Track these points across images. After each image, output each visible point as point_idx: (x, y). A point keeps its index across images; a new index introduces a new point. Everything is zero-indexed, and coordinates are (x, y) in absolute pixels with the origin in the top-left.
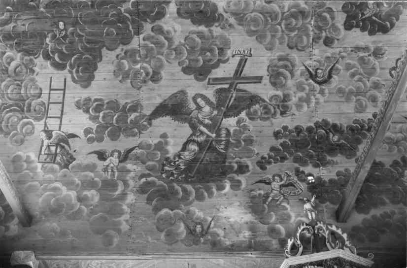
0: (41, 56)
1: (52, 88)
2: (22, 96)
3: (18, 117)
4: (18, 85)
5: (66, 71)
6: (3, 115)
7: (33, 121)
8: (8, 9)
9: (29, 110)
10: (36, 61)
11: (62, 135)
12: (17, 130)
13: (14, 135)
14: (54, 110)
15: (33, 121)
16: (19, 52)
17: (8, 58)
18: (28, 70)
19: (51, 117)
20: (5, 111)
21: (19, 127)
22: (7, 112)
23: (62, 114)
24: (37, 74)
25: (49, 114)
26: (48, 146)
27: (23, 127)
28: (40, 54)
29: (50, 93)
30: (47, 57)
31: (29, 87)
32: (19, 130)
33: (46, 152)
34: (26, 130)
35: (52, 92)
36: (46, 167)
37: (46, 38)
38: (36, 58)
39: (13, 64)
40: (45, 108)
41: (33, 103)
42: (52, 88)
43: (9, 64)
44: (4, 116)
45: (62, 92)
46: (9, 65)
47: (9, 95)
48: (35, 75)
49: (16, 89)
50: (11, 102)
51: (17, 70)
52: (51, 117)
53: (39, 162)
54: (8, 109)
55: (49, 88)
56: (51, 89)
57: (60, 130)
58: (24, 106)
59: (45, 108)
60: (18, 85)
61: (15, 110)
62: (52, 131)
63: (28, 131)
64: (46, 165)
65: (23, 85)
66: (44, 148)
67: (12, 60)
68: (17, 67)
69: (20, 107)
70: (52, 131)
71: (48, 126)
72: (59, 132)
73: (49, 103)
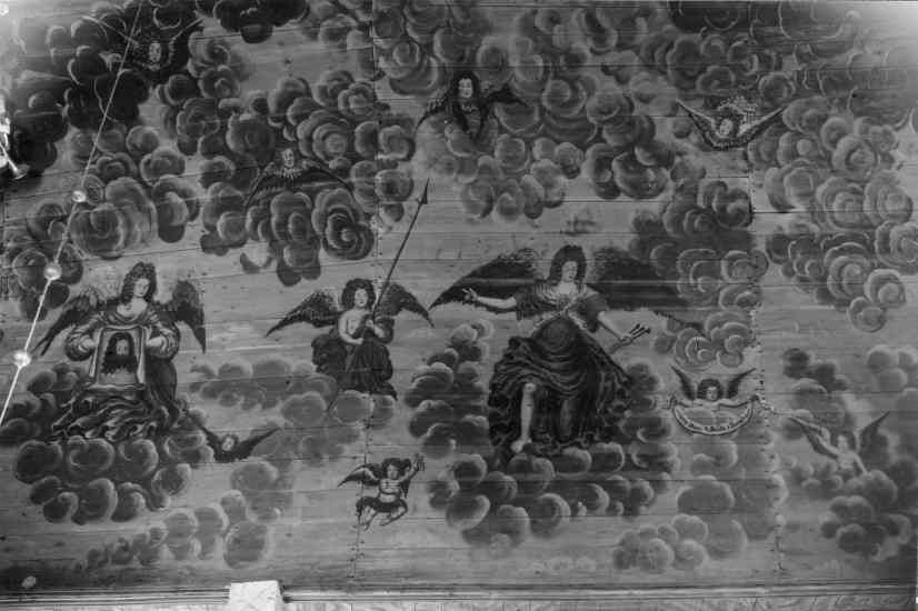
0: (910, 124)
2: (867, 218)
3: (862, 267)
4: (854, 191)
7: (898, 274)
9: (886, 250)
10: (897, 136)
12: (865, 297)
13: (860, 307)
15: (898, 274)
16: (859, 114)
17: (832, 129)
18: (879, 157)
21: (867, 287)
22: (836, 254)
24: (899, 168)
27: (877, 289)
28: (907, 120)
31: (880, 195)
32: (868, 293)
38: (897, 129)
39: (844, 144)
41: (894, 232)
43: (834, 143)
44: (829, 263)
46: (835, 147)
47: (837, 216)
48: (893, 169)
49: (850, 200)
50: (842, 232)
51: (853, 157)
54: (836, 248)
60: (854, 191)
61: (850, 250)
63: (890, 298)
65: (866, 191)
67: (842, 134)
68: (852, 151)
69: (863, 242)
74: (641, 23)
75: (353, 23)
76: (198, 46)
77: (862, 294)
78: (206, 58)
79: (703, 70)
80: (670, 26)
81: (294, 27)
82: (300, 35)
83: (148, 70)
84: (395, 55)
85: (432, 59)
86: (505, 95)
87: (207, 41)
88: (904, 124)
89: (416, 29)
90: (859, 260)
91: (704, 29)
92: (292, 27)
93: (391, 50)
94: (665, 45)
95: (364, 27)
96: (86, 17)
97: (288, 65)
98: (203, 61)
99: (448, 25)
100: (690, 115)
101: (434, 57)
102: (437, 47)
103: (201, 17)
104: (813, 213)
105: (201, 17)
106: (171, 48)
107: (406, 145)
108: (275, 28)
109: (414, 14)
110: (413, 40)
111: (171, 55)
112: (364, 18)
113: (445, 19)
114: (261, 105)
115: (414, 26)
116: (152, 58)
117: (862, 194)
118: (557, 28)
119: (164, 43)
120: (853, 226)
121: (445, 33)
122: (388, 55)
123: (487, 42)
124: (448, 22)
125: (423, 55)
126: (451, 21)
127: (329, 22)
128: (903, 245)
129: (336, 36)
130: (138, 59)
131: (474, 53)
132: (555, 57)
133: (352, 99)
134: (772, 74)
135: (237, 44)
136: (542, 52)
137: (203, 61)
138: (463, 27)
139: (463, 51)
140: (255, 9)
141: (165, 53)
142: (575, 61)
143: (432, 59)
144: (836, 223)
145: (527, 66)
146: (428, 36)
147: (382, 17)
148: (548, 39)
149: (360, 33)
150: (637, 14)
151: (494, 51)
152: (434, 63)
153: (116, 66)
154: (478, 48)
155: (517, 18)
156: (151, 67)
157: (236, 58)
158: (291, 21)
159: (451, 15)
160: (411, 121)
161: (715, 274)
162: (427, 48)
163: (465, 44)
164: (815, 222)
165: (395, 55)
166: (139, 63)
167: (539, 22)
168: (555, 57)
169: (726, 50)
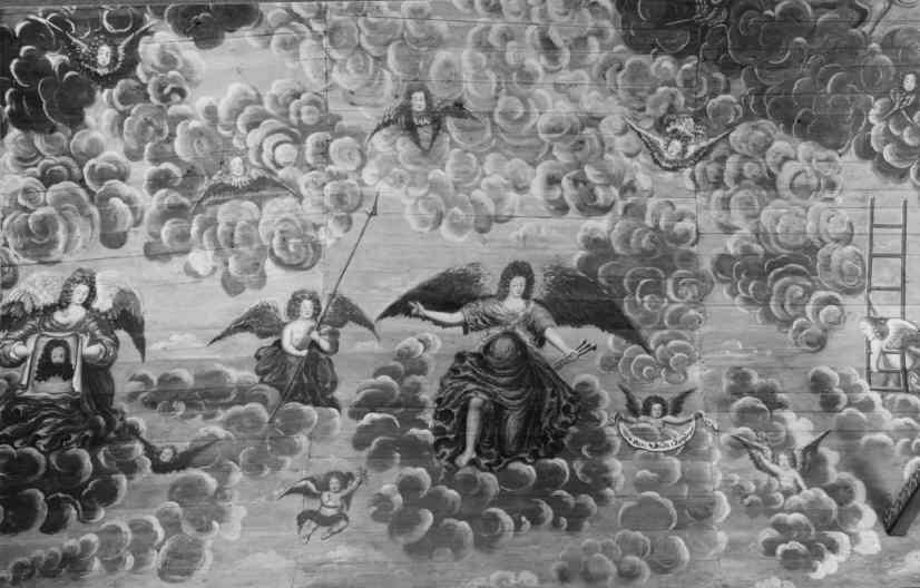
0: (852, 149)
1: (876, 222)
3: (804, 286)
5: (907, 185)
6: (769, 283)
7: (837, 295)
8: (798, 43)
11: (910, 330)
13: (801, 329)
14: (884, 274)
15: (837, 295)
19: (878, 289)
20: (772, 274)
23: (904, 282)
24: (841, 191)
25: (873, 279)
26: (884, 353)
28: (850, 146)
29: (871, 235)
30: (866, 152)
32: (809, 315)
33: (882, 367)
34: (826, 316)
35: (875, 230)
36: (892, 401)
37: (868, 111)
39: (789, 169)
40: (864, 269)
41: (835, 256)
42: (876, 222)
43: (780, 166)
44: (772, 285)
45: (900, 231)
47: (781, 238)
50: (785, 253)
51: (796, 181)
52: (878, 289)
53: (872, 390)
54: (780, 270)
55: (868, 222)
56: (873, 226)
57: (904, 318)
58: (815, 259)
59: (864, 269)
61: (796, 273)
62: (886, 320)
63: (832, 319)
64: (890, 396)
65: (809, 215)
66: (874, 358)
68: (798, 173)
69: (805, 263)
70: (886, 320)
71: (875, 307)
72: (900, 321)
73: (872, 256)
74: (593, 42)
76: (149, 50)
77: (804, 314)
78: (157, 64)
79: (653, 91)
80: (621, 47)
81: (248, 33)
82: (254, 43)
83: (96, 74)
85: (386, 72)
86: (458, 109)
87: (157, 45)
88: (847, 151)
90: (801, 283)
91: (654, 50)
92: (246, 36)
93: (345, 61)
94: (616, 65)
96: (32, 17)
98: (153, 66)
99: (403, 38)
100: (639, 134)
101: (388, 70)
104: (757, 235)
105: (150, 20)
106: (121, 51)
107: (358, 159)
108: (227, 34)
110: (367, 51)
111: (120, 59)
114: (211, 112)
115: (368, 38)
117: (805, 218)
118: (511, 44)
119: (115, 47)
120: (796, 248)
122: (343, 69)
124: (402, 35)
126: (406, 35)
127: (282, 30)
128: (844, 267)
129: (290, 45)
130: (86, 62)
132: (508, 74)
133: (305, 109)
134: (721, 97)
135: (188, 51)
136: (495, 68)
137: (153, 66)
138: (417, 41)
139: (418, 64)
140: (208, 14)
141: (114, 58)
142: (527, 78)
143: (386, 72)
144: (778, 243)
145: (479, 78)
146: (382, 48)
149: (314, 43)
150: (590, 34)
151: (447, 65)
153: (64, 68)
154: (431, 62)
156: (99, 71)
157: (186, 63)
158: (244, 28)
159: (405, 28)
160: (364, 134)
161: (661, 293)
162: (380, 60)
163: (418, 57)
164: (760, 243)
166: (87, 66)
167: (493, 38)
168: (508, 74)
169: (676, 73)
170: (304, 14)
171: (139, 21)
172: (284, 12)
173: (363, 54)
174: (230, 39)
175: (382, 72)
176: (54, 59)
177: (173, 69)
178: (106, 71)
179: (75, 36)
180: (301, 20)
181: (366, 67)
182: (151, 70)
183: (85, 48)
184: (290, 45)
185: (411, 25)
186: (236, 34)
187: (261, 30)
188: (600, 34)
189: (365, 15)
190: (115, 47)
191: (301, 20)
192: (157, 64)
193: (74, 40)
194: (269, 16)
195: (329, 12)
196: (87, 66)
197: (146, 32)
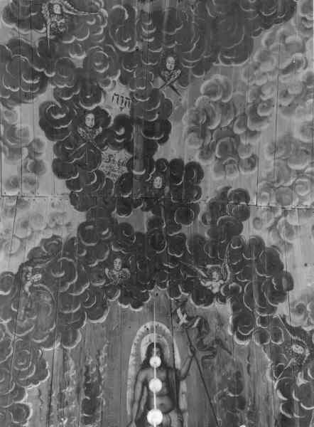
74: (289, 40)
75: (283, 219)
76: (296, 320)
78: (302, 317)
81: (284, 257)
83: (309, 357)
84: (303, 194)
85: (306, 171)
89: (286, 181)
92: (284, 258)
93: (299, 196)
95: (285, 213)
96: (275, 387)
97: (309, 265)
98: (304, 319)
99: (286, 160)
101: (306, 168)
102: (299, 167)
103: (277, 315)
105: (277, 315)
108: (285, 269)
109: (278, 181)
110: (294, 182)
112: (280, 212)
113: (282, 162)
116: (301, 353)
118: (290, 92)
119: (292, 342)
121: (291, 162)
122: (302, 199)
123: (298, 136)
124: (284, 160)
125: (304, 176)
126: (284, 158)
127: (282, 235)
129: (290, 231)
130: (302, 361)
131: (304, 144)
132: (308, 92)
135: (294, 295)
136: (305, 100)
137: (304, 319)
138: (288, 151)
141: (298, 343)
143: (306, 171)
146: (292, 174)
147: (279, 201)
148: (297, 97)
149: (288, 216)
150: (284, 43)
151: (303, 131)
152: (309, 169)
153: (306, 377)
155: (285, 117)
156: (307, 355)
157: (302, 298)
158: (281, 257)
162: (299, 173)
163: (297, 150)
165: (303, 194)
166: (304, 362)
167: (286, 103)
168: (308, 92)
170: (272, 221)
171: (276, 321)
172: (271, 233)
173: (296, 185)
174: (287, 268)
175: (307, 173)
176: (301, 381)
177: (305, 307)
178: (307, 351)
179: (287, 364)
180: (276, 223)
181: (302, 183)
182: (306, 321)
183: (293, 360)
184: (290, 231)
185: (279, 154)
186: (284, 263)
187: (282, 248)
188: (284, 37)
189: (273, 183)
190: (292, 342)
191: (276, 223)
192: (302, 317)
193: (289, 365)
194: (274, 242)
195: (271, 205)
196: (304, 362)
197: (284, 320)
